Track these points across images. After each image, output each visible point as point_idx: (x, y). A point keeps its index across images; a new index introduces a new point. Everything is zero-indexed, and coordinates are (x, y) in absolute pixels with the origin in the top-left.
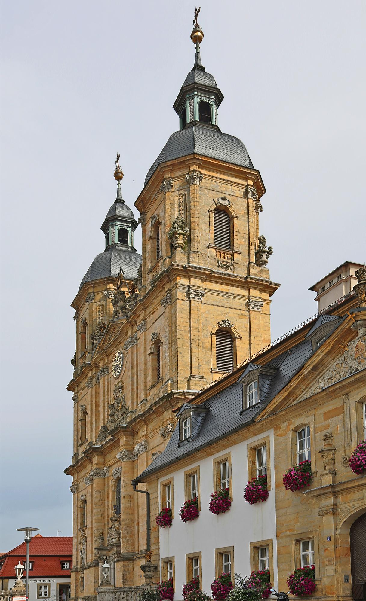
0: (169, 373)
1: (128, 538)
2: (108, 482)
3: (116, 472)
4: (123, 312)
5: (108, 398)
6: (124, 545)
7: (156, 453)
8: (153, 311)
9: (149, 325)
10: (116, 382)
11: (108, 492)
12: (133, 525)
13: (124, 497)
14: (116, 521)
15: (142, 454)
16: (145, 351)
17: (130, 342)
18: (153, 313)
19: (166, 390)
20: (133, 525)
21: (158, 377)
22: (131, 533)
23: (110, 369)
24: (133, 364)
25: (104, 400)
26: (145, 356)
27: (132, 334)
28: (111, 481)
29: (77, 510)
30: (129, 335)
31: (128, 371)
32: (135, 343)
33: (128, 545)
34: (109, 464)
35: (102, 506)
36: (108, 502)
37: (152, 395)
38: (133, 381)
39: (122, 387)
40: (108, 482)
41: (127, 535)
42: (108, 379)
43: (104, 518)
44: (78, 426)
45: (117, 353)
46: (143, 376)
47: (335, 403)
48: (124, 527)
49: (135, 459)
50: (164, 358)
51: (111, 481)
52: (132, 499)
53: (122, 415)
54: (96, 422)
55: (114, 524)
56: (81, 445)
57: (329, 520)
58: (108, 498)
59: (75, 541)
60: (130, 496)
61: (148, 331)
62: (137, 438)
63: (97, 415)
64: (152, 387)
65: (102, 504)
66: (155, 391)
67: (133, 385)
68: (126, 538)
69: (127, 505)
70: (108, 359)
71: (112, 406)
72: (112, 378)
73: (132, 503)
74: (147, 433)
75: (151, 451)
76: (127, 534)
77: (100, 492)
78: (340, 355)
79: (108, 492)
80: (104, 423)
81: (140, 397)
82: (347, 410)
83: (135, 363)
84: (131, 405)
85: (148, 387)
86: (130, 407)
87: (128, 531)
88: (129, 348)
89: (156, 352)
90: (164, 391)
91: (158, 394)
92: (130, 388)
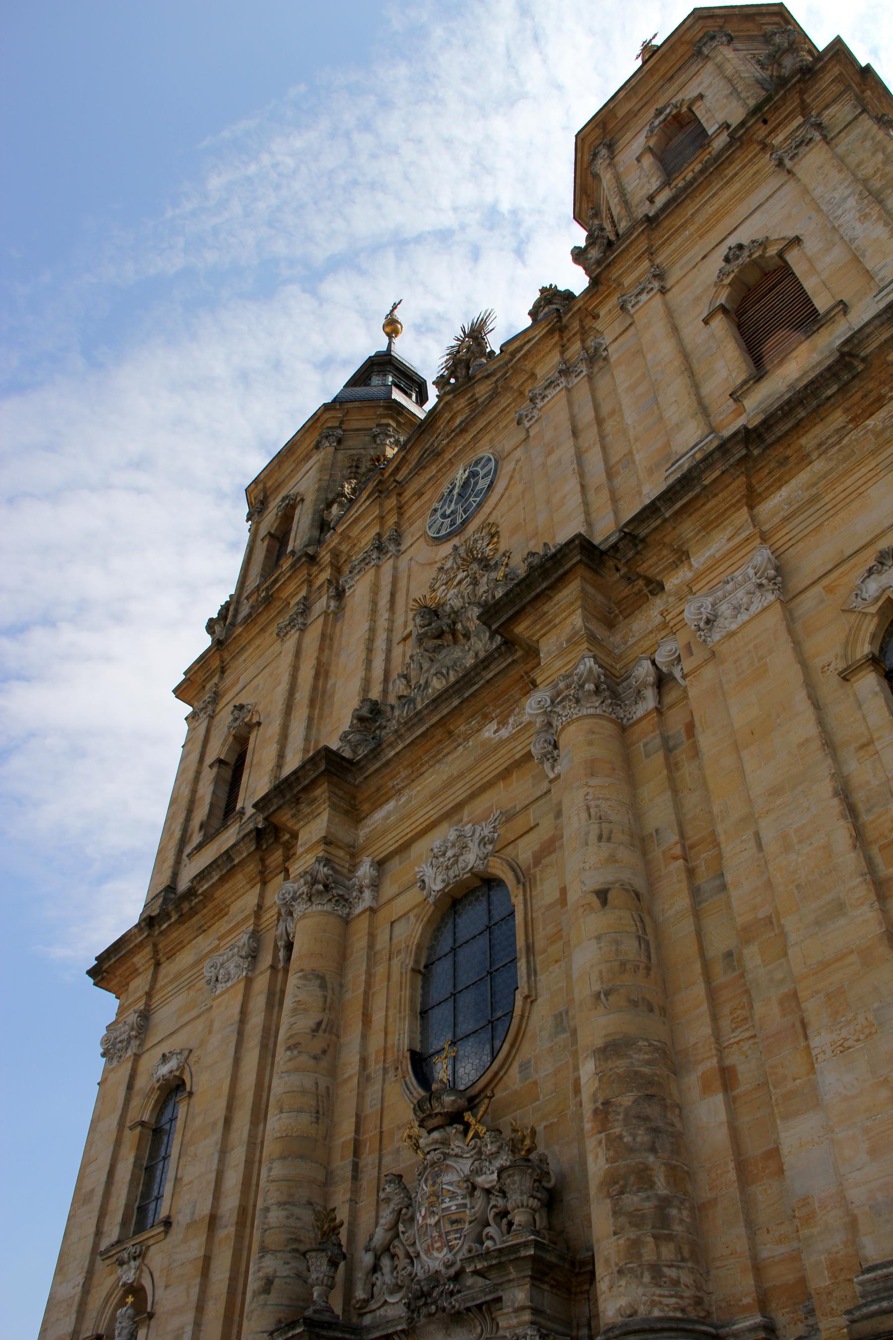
1: (662, 1187)
5: (391, 621)
6: (634, 1247)
11: (368, 985)
25: (372, 630)
28: (392, 923)
33: (668, 1252)
35: (324, 1064)
36: (364, 1037)
41: (651, 1158)
42: (395, 568)
48: (627, 1100)
49: (639, 714)
51: (392, 923)
54: (309, 727)
65: (324, 1052)
68: (652, 1185)
76: (653, 1149)
77: (323, 986)
79: (368, 985)
87: (655, 1131)
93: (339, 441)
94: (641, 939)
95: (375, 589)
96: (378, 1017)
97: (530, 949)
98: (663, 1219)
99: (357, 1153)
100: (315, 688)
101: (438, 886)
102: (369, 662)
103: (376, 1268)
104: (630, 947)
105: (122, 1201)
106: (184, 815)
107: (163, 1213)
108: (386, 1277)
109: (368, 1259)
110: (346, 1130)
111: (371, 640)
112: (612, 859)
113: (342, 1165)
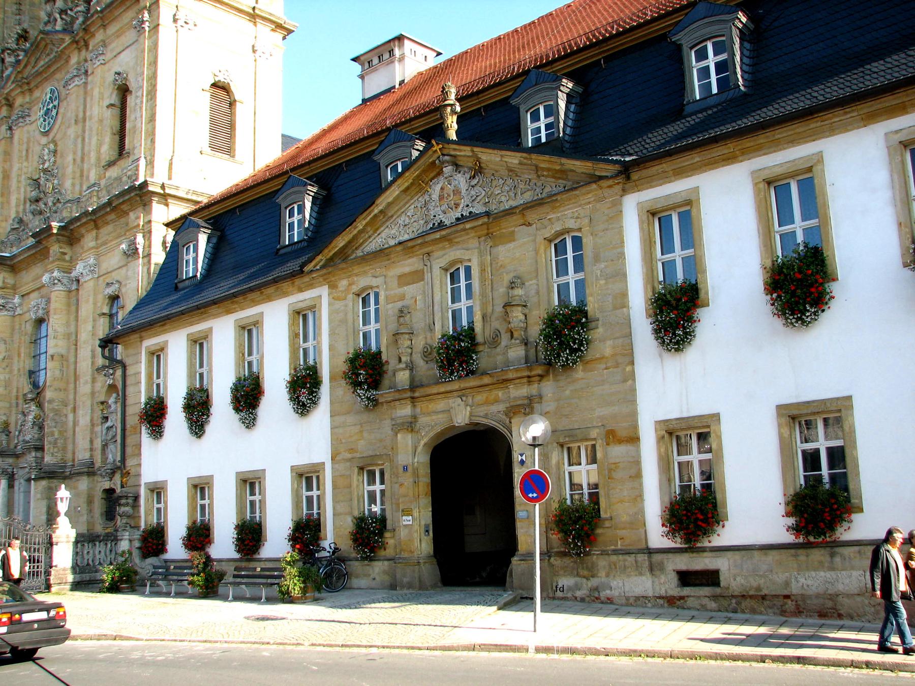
2: (20, 324)
4: (62, 19)
7: (112, 283)
8: (119, 34)
10: (44, 140)
12: (65, 412)
14: (32, 400)
15: (88, 280)
16: (102, 98)
17: (75, 76)
18: (118, 37)
19: (135, 174)
20: (65, 412)
21: (121, 150)
22: (62, 427)
24: (77, 116)
30: (74, 65)
31: (69, 127)
34: (24, 289)
35: (7, 370)
36: (18, 361)
37: (110, 178)
38: (76, 146)
39: (55, 152)
40: (20, 324)
43: (10, 392)
45: (48, 90)
47: (409, 265)
50: (133, 117)
52: (65, 363)
53: (54, 204)
57: (405, 440)
58: (19, 355)
60: (62, 356)
61: (107, 65)
62: (77, 248)
64: (111, 164)
66: (113, 172)
67: (75, 153)
69: (57, 373)
70: (31, 95)
71: (36, 183)
72: (37, 132)
73: (65, 369)
74: (97, 244)
75: (104, 277)
78: (420, 194)
80: (17, 212)
81: (88, 177)
82: (427, 276)
83: (81, 115)
84: (70, 188)
85: (103, 163)
86: (69, 192)
89: (118, 103)
90: (132, 176)
91: (119, 179)
92: (70, 158)
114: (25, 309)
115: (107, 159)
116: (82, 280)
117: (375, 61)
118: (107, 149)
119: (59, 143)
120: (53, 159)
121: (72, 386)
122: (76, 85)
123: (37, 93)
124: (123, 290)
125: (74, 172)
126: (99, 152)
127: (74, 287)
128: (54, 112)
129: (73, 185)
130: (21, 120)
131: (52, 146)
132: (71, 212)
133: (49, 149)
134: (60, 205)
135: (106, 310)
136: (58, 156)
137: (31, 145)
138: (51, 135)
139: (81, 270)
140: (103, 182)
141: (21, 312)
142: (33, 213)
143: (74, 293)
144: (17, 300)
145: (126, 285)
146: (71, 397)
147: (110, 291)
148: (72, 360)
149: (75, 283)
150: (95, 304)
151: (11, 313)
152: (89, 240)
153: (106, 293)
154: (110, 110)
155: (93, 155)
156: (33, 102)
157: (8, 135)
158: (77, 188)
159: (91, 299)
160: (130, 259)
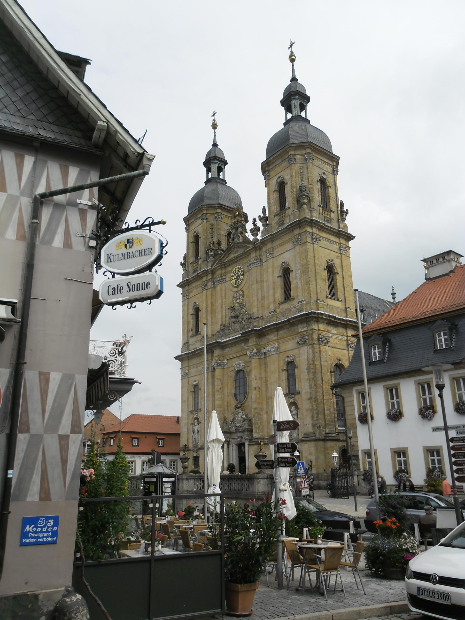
0: (302, 295)
1: (259, 425)
3: (238, 365)
7: (290, 356)
9: (275, 254)
10: (235, 290)
13: (255, 388)
14: (240, 407)
18: (281, 246)
19: (301, 308)
23: (227, 277)
24: (257, 280)
25: (222, 302)
26: (273, 276)
27: (256, 257)
29: (188, 393)
31: (252, 285)
32: (259, 264)
34: (229, 357)
36: (227, 389)
37: (282, 309)
39: (243, 296)
42: (225, 286)
44: (188, 319)
45: (237, 267)
46: (271, 292)
49: (262, 357)
55: (239, 411)
56: (192, 336)
58: (228, 386)
59: (183, 422)
60: (259, 388)
63: (213, 312)
64: (282, 303)
71: (233, 309)
72: (231, 286)
76: (259, 420)
77: (221, 381)
80: (222, 322)
81: (268, 308)
83: (259, 279)
84: (256, 312)
85: (278, 302)
86: (255, 314)
88: (253, 266)
92: (255, 298)
93: (207, 219)
94: (260, 395)
95: (221, 289)
96: (229, 386)
97: (249, 386)
98: (259, 427)
99: (228, 407)
100: (211, 309)
101: (236, 369)
102: (222, 311)
103: (231, 423)
104: (258, 396)
105: (191, 404)
106: (187, 325)
107: (200, 407)
108: (233, 425)
109: (230, 422)
110: (226, 403)
111: (222, 305)
112: (257, 383)
113: (226, 408)
114: (230, 365)
115: (280, 300)
116: (267, 354)
117: (435, 261)
118: (279, 294)
119: (245, 291)
120: (242, 298)
121: (265, 402)
122: (256, 266)
123: (229, 269)
124: (297, 359)
125: (258, 305)
126: (274, 297)
127: (263, 356)
128: (241, 277)
129: (258, 310)
130: (221, 280)
131: (241, 293)
132: (259, 323)
133: (239, 294)
134: (252, 320)
135: (285, 368)
136: (245, 297)
137: (227, 291)
138: (240, 288)
139: (270, 350)
140: (278, 311)
141: (227, 367)
142: (234, 323)
143: (262, 359)
144: (226, 361)
145: (299, 357)
146: (265, 406)
147: (289, 360)
148: (264, 389)
149: (263, 355)
150: (279, 365)
151: (222, 367)
152: (272, 337)
153: (286, 360)
154: (279, 278)
155: (271, 299)
156: (227, 272)
157: (212, 287)
158: (260, 312)
159: (277, 363)
160: (301, 346)
